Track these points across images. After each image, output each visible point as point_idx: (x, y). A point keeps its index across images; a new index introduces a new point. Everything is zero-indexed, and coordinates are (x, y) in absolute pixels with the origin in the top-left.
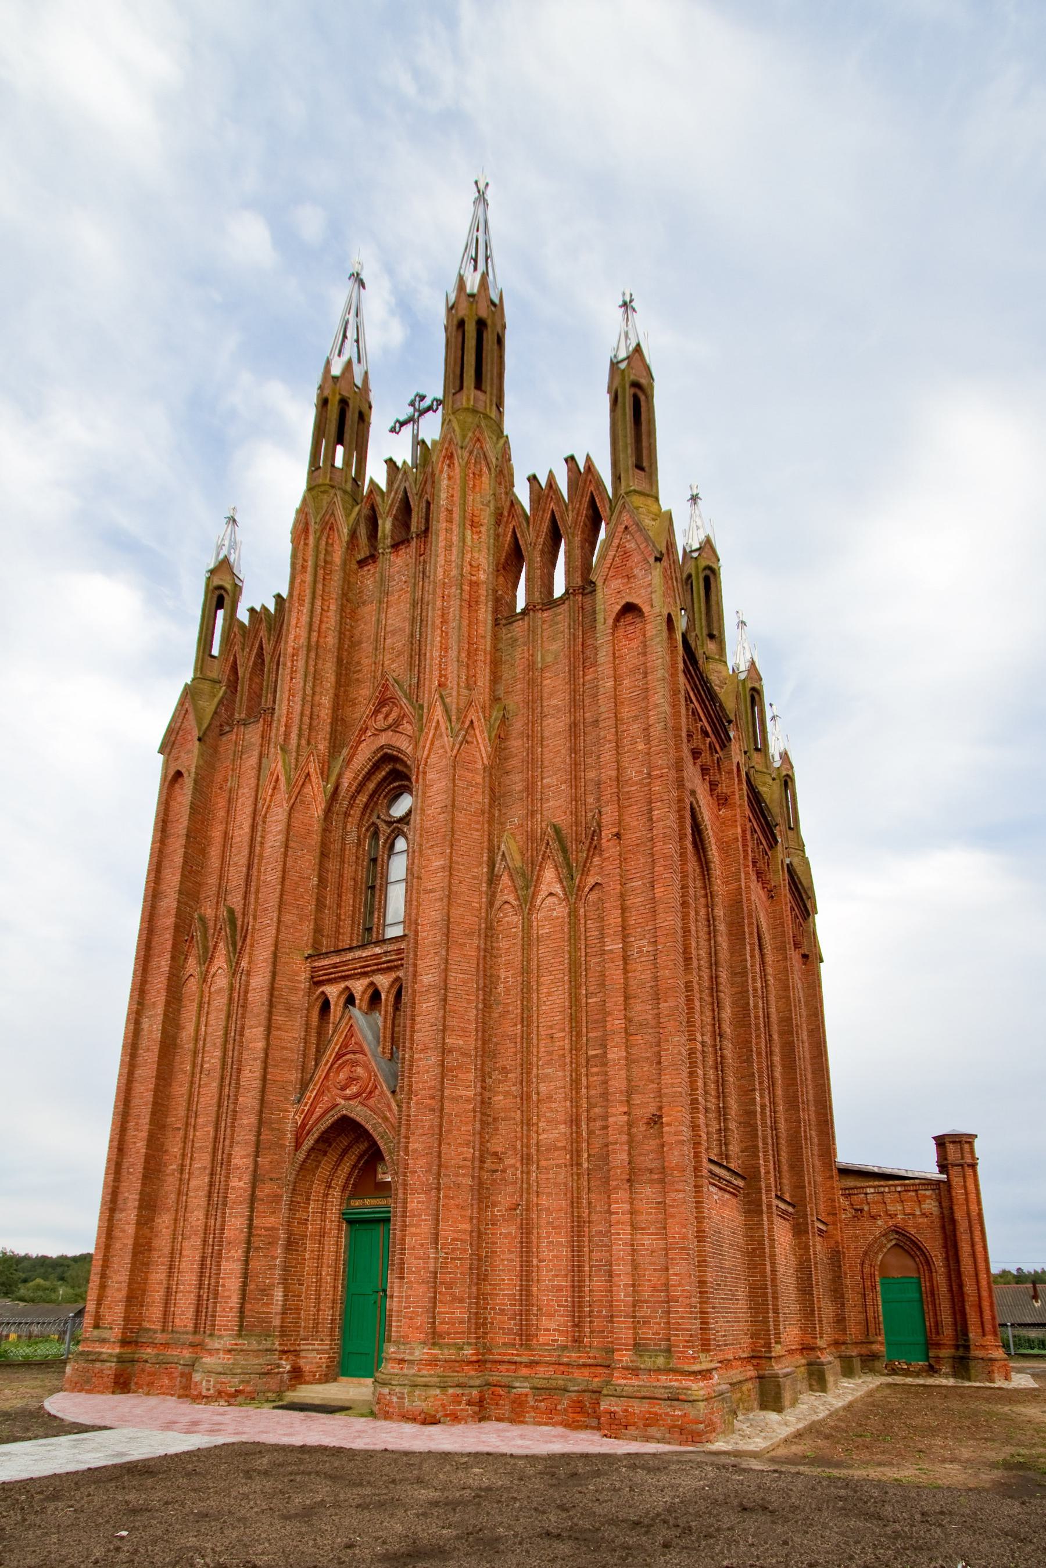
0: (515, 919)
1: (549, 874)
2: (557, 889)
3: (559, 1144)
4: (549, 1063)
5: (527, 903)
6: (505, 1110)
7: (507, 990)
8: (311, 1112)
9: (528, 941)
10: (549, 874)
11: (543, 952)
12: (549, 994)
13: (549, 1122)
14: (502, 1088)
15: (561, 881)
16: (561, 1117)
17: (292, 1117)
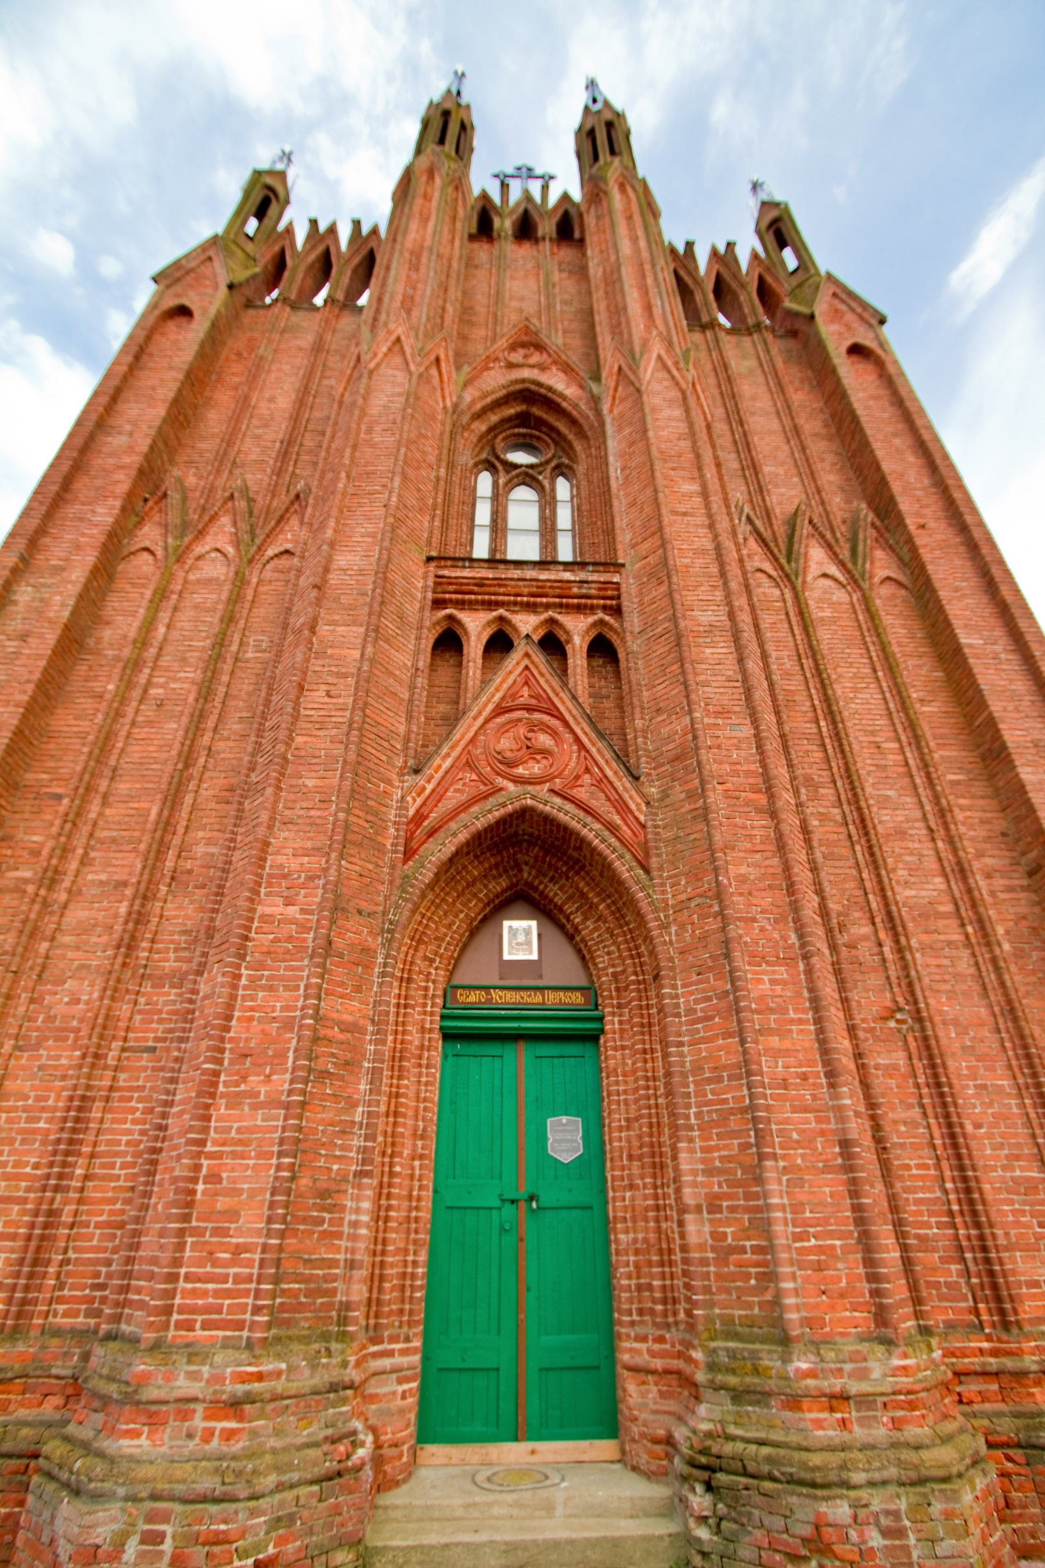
3: (942, 909)
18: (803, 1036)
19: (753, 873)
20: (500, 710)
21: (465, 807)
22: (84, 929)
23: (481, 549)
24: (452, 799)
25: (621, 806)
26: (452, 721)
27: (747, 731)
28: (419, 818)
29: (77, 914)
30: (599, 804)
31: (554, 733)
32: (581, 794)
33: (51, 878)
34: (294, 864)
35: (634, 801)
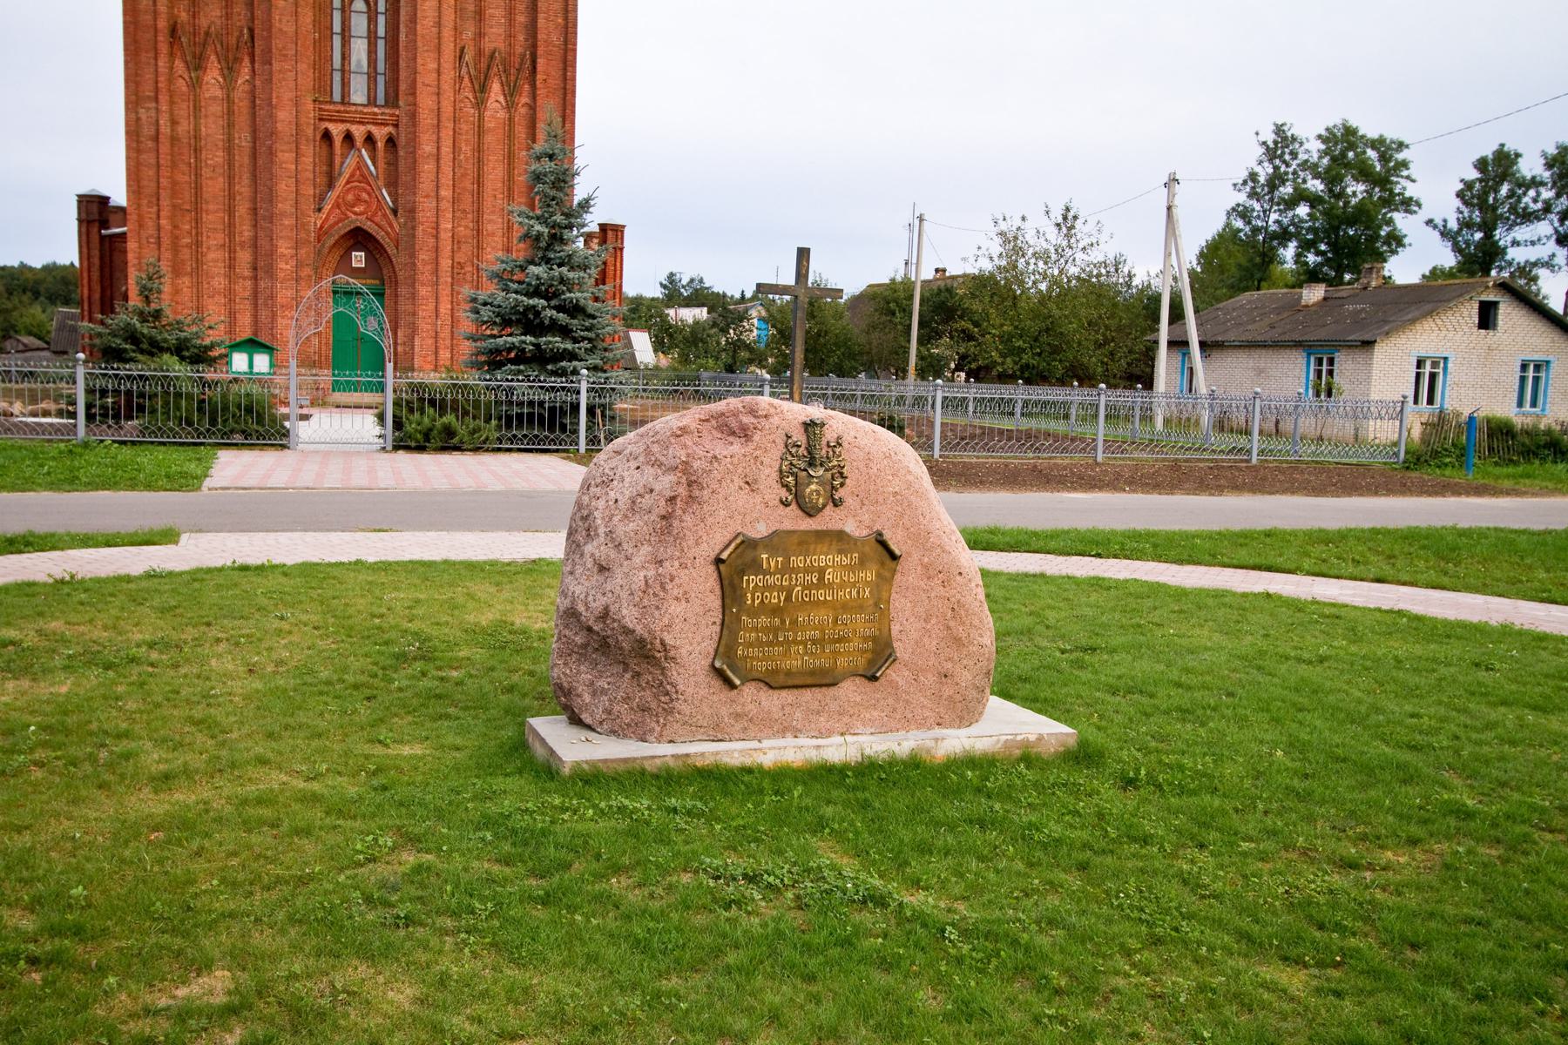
0: (472, 111)
1: (496, 87)
2: (501, 99)
4: (493, 212)
5: (480, 104)
6: (465, 236)
7: (467, 159)
8: (327, 219)
9: (480, 130)
10: (496, 87)
13: (493, 248)
15: (505, 95)
16: (500, 246)
17: (314, 221)
18: (432, 306)
19: (426, 258)
20: (348, 182)
21: (336, 223)
24: (331, 221)
25: (391, 225)
26: (331, 185)
27: (434, 204)
28: (321, 227)
29: (211, 256)
30: (383, 223)
31: (369, 194)
32: (377, 219)
33: (198, 244)
34: (286, 252)
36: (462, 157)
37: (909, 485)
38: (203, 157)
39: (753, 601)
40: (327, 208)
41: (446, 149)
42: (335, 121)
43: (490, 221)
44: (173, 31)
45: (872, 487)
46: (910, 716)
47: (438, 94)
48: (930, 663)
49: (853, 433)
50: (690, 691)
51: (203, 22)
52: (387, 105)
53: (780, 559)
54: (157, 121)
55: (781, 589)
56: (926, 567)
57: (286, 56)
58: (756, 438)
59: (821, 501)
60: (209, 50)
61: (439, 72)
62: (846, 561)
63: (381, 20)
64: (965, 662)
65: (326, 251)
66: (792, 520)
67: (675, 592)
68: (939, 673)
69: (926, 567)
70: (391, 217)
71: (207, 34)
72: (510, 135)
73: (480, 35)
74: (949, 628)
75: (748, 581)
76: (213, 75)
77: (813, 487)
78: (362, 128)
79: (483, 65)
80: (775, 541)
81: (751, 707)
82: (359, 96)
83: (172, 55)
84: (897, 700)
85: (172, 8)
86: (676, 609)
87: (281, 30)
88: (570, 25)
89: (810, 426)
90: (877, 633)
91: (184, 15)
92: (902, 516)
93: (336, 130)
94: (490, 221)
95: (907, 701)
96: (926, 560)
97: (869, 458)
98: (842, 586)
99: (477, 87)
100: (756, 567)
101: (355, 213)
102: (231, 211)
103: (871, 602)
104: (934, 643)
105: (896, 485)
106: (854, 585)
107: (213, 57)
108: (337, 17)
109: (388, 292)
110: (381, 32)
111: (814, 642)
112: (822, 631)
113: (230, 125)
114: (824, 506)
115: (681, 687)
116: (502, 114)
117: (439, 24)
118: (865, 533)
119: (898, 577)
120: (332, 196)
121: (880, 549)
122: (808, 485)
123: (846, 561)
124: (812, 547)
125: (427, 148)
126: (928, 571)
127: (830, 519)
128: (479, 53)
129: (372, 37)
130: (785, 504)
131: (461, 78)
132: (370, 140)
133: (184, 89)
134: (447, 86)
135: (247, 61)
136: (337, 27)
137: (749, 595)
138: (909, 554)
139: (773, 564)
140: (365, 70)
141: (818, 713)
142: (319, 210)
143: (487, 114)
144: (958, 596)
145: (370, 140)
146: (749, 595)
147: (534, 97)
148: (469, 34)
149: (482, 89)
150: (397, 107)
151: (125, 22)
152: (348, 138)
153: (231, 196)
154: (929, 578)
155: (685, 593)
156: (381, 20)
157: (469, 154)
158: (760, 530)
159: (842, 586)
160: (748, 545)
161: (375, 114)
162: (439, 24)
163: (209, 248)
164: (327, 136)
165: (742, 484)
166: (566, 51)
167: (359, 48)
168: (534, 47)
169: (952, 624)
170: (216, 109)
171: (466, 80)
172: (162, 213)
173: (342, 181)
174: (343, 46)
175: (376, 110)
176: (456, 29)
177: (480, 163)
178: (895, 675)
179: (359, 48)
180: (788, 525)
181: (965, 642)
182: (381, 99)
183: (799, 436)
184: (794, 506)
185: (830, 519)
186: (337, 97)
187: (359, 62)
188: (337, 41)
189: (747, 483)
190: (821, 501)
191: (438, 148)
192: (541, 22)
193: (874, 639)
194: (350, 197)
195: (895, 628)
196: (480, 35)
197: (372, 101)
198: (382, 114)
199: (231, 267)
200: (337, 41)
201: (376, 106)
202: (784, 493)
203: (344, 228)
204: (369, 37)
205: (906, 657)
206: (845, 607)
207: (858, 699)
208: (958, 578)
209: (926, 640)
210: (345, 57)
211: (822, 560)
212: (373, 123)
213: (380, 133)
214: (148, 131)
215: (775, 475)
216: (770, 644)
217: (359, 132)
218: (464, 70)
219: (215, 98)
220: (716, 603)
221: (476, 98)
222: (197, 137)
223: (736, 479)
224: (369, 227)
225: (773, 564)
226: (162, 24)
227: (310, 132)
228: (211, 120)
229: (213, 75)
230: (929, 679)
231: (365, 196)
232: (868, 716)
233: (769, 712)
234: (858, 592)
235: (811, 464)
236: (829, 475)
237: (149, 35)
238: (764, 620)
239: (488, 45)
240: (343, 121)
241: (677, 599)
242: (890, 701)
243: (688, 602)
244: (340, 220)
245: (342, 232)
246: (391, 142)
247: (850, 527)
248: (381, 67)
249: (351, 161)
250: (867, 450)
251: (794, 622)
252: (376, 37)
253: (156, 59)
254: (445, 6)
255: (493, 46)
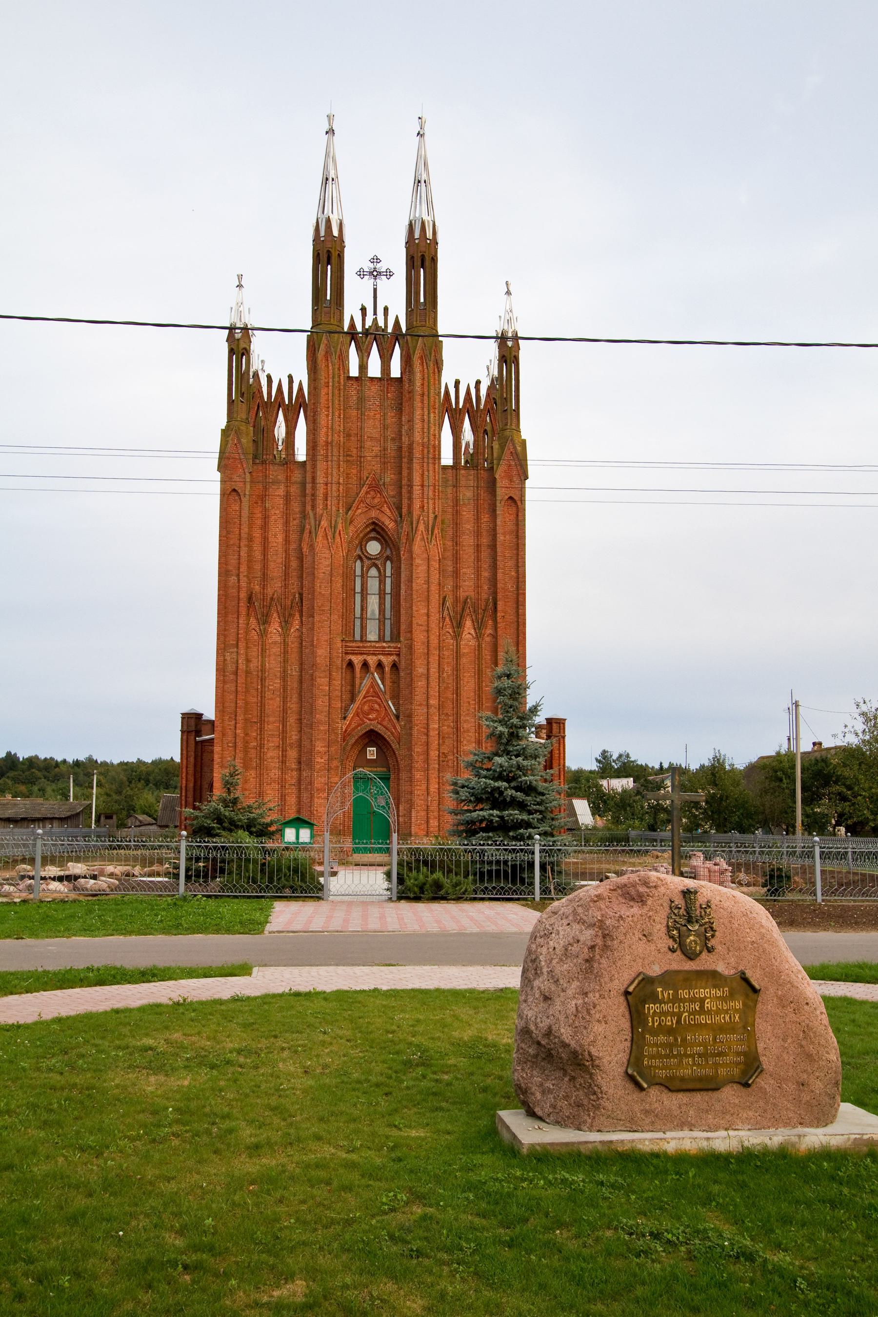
1: (468, 623)
2: (472, 632)
4: (468, 714)
5: (457, 636)
7: (448, 676)
9: (458, 655)
10: (468, 623)
11: (464, 660)
12: (468, 682)
14: (446, 723)
15: (475, 629)
17: (342, 726)
18: (424, 787)
20: (364, 697)
22: (272, 758)
23: (357, 637)
24: (353, 726)
25: (395, 728)
26: (353, 700)
27: (425, 710)
28: (346, 731)
29: (270, 754)
30: (389, 726)
31: (379, 705)
32: (385, 723)
33: (261, 746)
34: (321, 750)
35: (398, 727)
36: (445, 675)
37: (763, 936)
38: (267, 684)
39: (653, 1023)
40: (350, 716)
41: (434, 670)
42: (356, 654)
43: (465, 721)
44: (250, 599)
45: (735, 938)
46: (777, 1116)
47: (428, 631)
48: (790, 1074)
49: (718, 898)
50: (611, 1091)
51: (270, 591)
52: (392, 641)
53: (671, 992)
54: (237, 661)
55: (673, 1014)
56: (780, 999)
57: (323, 610)
58: (649, 902)
59: (698, 948)
60: (273, 609)
61: (428, 615)
62: (719, 993)
63: (388, 581)
64: (817, 1074)
65: (349, 748)
66: (678, 963)
67: (597, 1016)
68: (797, 1082)
69: (780, 999)
70: (395, 721)
71: (272, 599)
72: (479, 657)
73: (456, 587)
74: (802, 1046)
75: (649, 1008)
76: (275, 627)
77: (692, 938)
78: (375, 658)
79: (459, 609)
80: (668, 978)
81: (656, 1105)
82: (372, 636)
83: (248, 615)
84: (767, 1103)
85: (250, 583)
86: (599, 1028)
87: (320, 593)
88: (521, 576)
89: (687, 894)
90: (747, 1049)
91: (257, 587)
92: (759, 959)
93: (357, 660)
94: (465, 721)
95: (775, 1104)
96: (780, 993)
97: (731, 916)
98: (718, 1012)
99: (455, 624)
100: (654, 998)
101: (370, 720)
102: (284, 721)
103: (740, 1025)
104: (791, 1058)
105: (752, 936)
106: (726, 1012)
107: (275, 615)
108: (358, 581)
109: (392, 777)
110: (388, 589)
111: (700, 1055)
112: (706, 1048)
113: (285, 661)
114: (701, 952)
115: (604, 1088)
116: (473, 643)
117: (428, 582)
118: (732, 972)
119: (759, 1006)
120: (354, 707)
121: (744, 984)
122: (688, 936)
123: (719, 994)
124: (694, 983)
125: (421, 670)
126: (783, 1001)
127: (705, 962)
128: (456, 600)
129: (382, 594)
130: (673, 951)
131: (444, 618)
132: (380, 666)
133: (256, 637)
134: (434, 626)
135: (297, 616)
136: (358, 588)
137: (650, 1019)
138: (767, 989)
139: (666, 996)
140: (377, 617)
141: (707, 1111)
142: (345, 718)
143: (463, 643)
144: (807, 1022)
145: (380, 666)
146: (650, 1019)
147: (496, 629)
148: (449, 587)
149: (459, 625)
150: (400, 642)
151: (219, 595)
152: (365, 665)
153: (285, 711)
154: (783, 1007)
155: (604, 1017)
156: (388, 581)
157: (450, 672)
158: (655, 970)
159: (718, 1012)
160: (647, 981)
161: (384, 647)
162: (428, 582)
163: (268, 749)
164: (350, 664)
165: (641, 936)
166: (518, 594)
167: (373, 602)
168: (495, 594)
169: (804, 1043)
170: (276, 650)
171: (447, 619)
172: (238, 725)
173: (360, 697)
174: (362, 601)
175: (384, 644)
176: (440, 584)
177: (458, 679)
178: (764, 1083)
179: (373, 602)
180: (675, 967)
181: (816, 1058)
182: (388, 638)
183: (679, 901)
184: (679, 952)
185: (705, 962)
186: (358, 637)
187: (373, 611)
188: (358, 598)
189: (644, 935)
190: (698, 948)
191: (428, 670)
192: (500, 576)
193: (745, 1054)
194: (366, 708)
195: (761, 1046)
196: (456, 587)
197: (381, 638)
198: (389, 647)
199: (283, 762)
200: (358, 598)
201: (384, 642)
202: (671, 943)
203: (361, 730)
204: (380, 594)
205: (771, 1068)
206: (721, 1029)
207: (737, 1101)
208: (806, 1007)
209: (785, 1056)
210: (363, 609)
211: (702, 993)
212: (382, 654)
213: (387, 661)
214: (230, 668)
215: (664, 929)
216: (667, 1056)
217: (372, 660)
218: (446, 612)
219: (275, 643)
220: (626, 1024)
221: (454, 632)
222: (263, 670)
223: (636, 932)
224: (379, 729)
225: (666, 996)
226: (243, 595)
227: (339, 662)
228: (272, 658)
229: (275, 627)
230: (790, 1087)
231: (376, 706)
232: (745, 1115)
233: (670, 1110)
234: (730, 1018)
235: (690, 921)
236: (703, 929)
237: (234, 603)
238: (662, 1038)
239: (462, 594)
240: (361, 654)
241: (599, 1021)
242: (761, 1103)
243: (606, 1023)
244: (359, 725)
245: (360, 734)
246: (395, 666)
247: (721, 968)
248: (388, 614)
249: (367, 682)
250: (729, 910)
251: (684, 1040)
252: (385, 594)
253: (238, 618)
254: (432, 569)
255: (467, 594)
